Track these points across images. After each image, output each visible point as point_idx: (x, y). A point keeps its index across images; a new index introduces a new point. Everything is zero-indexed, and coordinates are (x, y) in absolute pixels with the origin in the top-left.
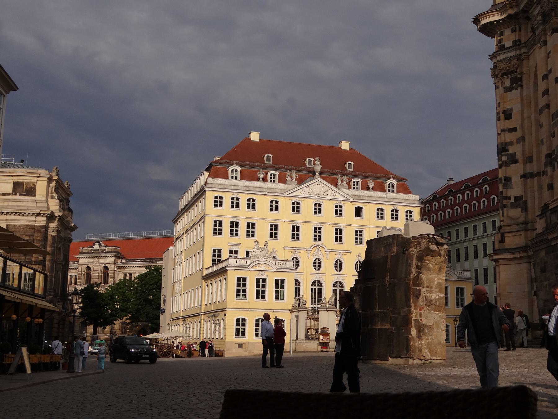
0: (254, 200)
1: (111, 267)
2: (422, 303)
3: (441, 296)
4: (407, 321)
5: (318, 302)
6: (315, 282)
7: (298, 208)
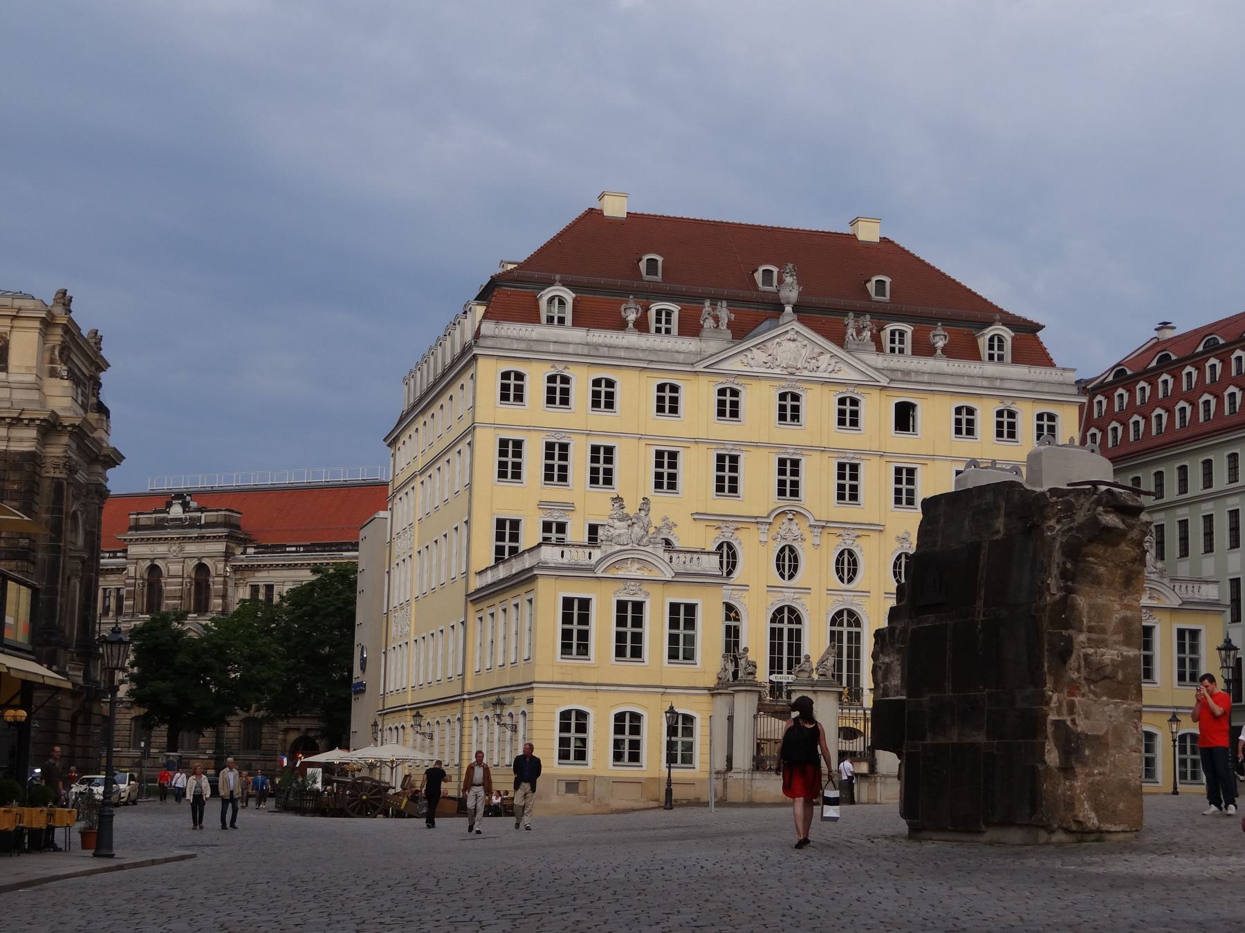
0: (610, 383)
1: (217, 567)
2: (1076, 673)
3: (1129, 656)
4: (1033, 724)
5: (790, 667)
6: (780, 610)
7: (735, 404)
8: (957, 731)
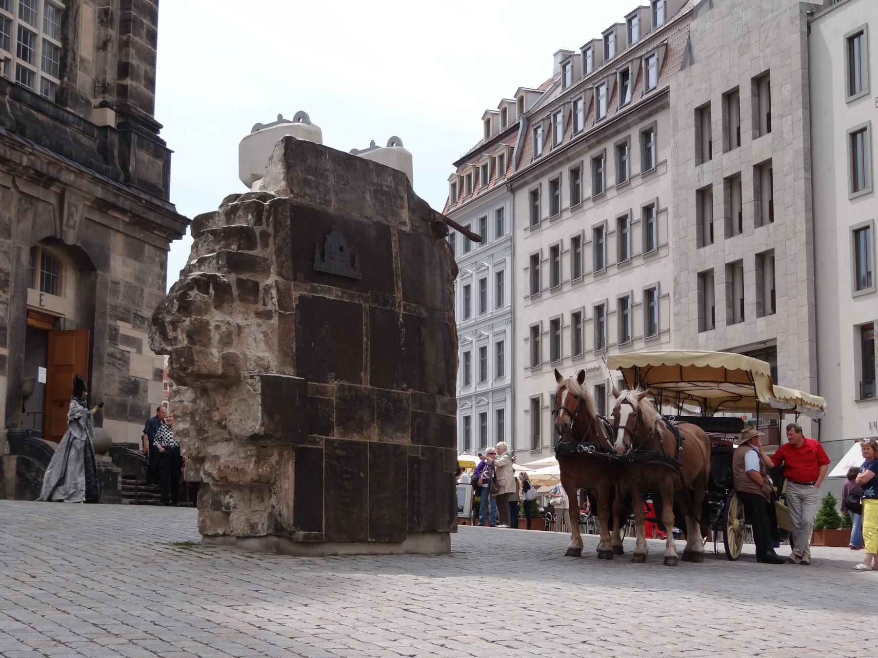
8: (377, 430)
